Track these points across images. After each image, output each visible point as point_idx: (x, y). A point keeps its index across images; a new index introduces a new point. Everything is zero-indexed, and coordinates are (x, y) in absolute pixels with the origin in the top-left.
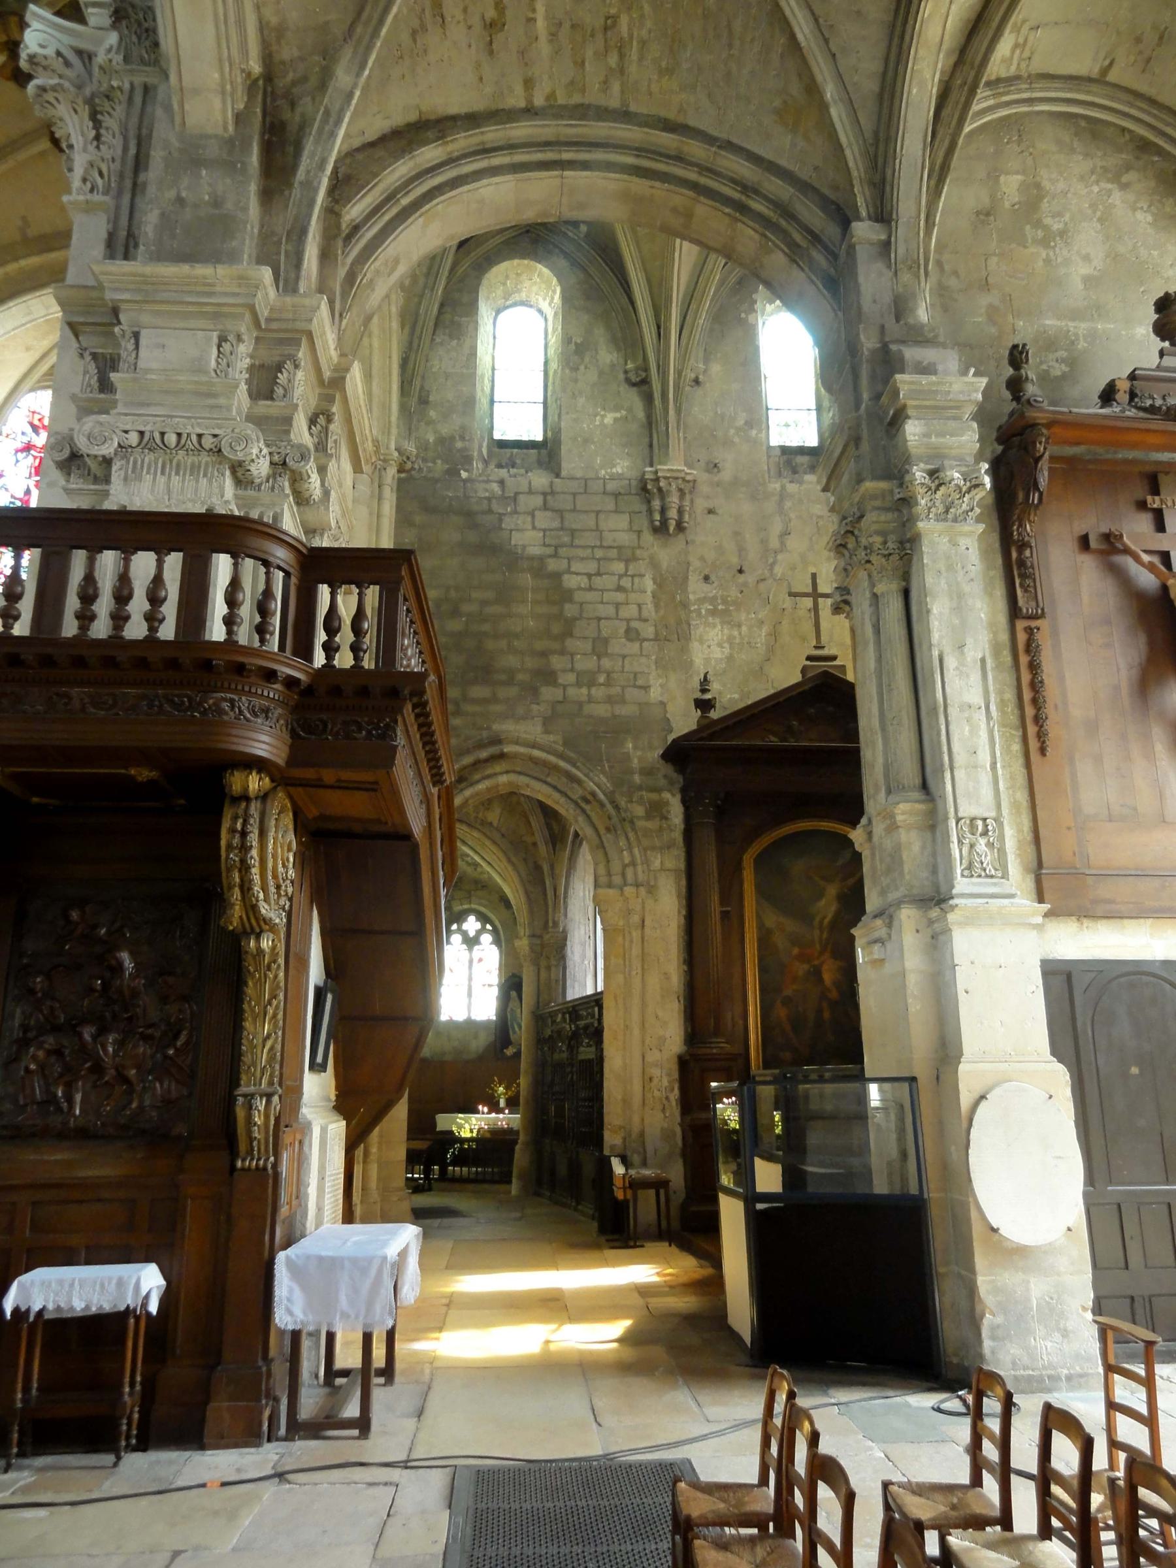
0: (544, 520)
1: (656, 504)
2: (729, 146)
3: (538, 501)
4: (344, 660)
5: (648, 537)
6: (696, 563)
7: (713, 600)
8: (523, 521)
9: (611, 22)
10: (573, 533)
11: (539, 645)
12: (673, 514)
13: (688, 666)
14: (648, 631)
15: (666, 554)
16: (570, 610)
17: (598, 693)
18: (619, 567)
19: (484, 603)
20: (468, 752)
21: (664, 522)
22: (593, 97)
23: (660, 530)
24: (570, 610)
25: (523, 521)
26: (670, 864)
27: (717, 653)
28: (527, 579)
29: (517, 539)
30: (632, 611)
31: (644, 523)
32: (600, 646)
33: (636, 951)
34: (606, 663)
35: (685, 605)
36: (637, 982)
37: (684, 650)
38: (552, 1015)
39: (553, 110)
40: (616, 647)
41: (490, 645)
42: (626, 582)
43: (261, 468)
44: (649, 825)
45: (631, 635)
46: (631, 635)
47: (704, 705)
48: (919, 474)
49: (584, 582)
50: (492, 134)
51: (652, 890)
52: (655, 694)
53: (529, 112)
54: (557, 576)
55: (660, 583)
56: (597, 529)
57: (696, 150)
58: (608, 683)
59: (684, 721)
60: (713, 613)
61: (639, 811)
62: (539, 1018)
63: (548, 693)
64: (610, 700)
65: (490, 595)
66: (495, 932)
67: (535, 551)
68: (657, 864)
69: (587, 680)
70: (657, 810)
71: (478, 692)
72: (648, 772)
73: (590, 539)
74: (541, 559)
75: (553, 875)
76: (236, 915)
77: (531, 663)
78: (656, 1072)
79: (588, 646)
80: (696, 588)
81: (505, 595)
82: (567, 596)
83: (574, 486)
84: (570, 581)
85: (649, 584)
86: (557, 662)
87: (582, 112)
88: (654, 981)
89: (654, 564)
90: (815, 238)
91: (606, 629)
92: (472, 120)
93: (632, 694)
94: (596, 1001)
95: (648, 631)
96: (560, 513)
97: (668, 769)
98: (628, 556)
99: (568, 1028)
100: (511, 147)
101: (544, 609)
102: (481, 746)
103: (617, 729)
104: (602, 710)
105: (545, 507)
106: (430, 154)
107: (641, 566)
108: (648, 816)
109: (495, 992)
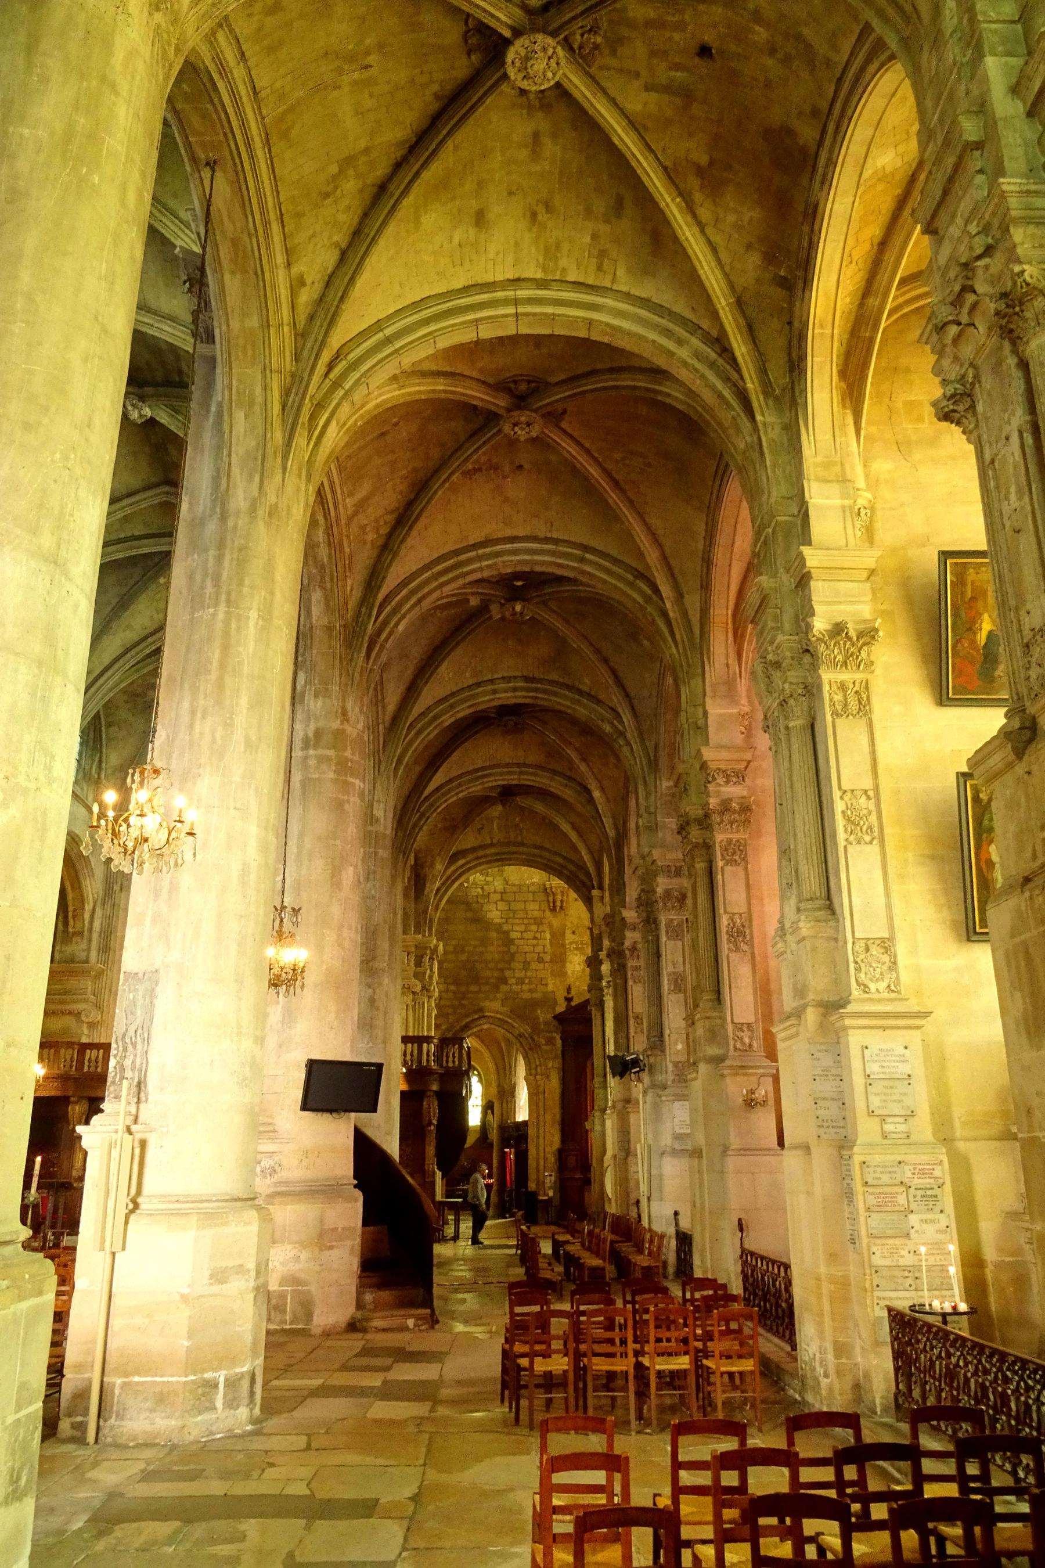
0: (502, 906)
1: (551, 899)
2: (556, 853)
3: (498, 897)
4: (451, 1065)
5: (548, 913)
6: (569, 925)
7: (576, 943)
8: (492, 907)
9: (517, 825)
10: (514, 912)
11: (500, 966)
12: (558, 904)
13: (563, 974)
14: (547, 958)
15: (555, 922)
16: (513, 949)
17: (525, 987)
18: (534, 928)
19: (475, 946)
20: (467, 1016)
21: (554, 907)
22: (512, 839)
23: (553, 909)
24: (513, 949)
25: (492, 907)
26: (556, 1065)
27: (578, 968)
28: (494, 935)
29: (490, 915)
30: (540, 949)
31: (545, 906)
32: (526, 965)
33: (541, 1104)
34: (529, 974)
35: (563, 946)
36: (541, 1118)
37: (564, 966)
38: (509, 1127)
39: (501, 844)
40: (533, 966)
41: (478, 966)
42: (538, 935)
43: (418, 989)
44: (548, 1048)
45: (540, 960)
46: (540, 960)
47: (569, 1000)
48: (604, 983)
49: (519, 935)
50: (481, 853)
51: (548, 1076)
52: (550, 988)
53: (492, 845)
54: (507, 933)
55: (553, 935)
56: (525, 910)
57: (546, 854)
58: (530, 983)
59: (561, 1008)
60: (577, 949)
61: (543, 1042)
62: (503, 1128)
63: (504, 988)
64: (530, 991)
65: (477, 943)
66: (479, 1075)
67: (497, 921)
68: (550, 1065)
69: (521, 981)
70: (550, 1041)
71: (473, 988)
72: (546, 1023)
73: (522, 915)
74: (500, 925)
75: (509, 1053)
76: (426, 1122)
77: (496, 974)
78: (549, 1156)
79: (521, 966)
80: (569, 937)
81: (484, 941)
82: (512, 942)
83: (515, 889)
84: (514, 935)
85: (548, 936)
86: (507, 973)
87: (509, 844)
88: (548, 1117)
89: (551, 926)
90: (584, 884)
91: (529, 957)
92: (474, 849)
93: (540, 988)
94: (525, 1123)
95: (547, 958)
96: (509, 902)
97: (556, 1023)
98: (538, 922)
99: (515, 1134)
100: (485, 856)
101: (502, 949)
102: (475, 1012)
103: (534, 1004)
104: (526, 996)
105: (502, 900)
106: (461, 862)
107: (545, 927)
108: (547, 1044)
109: (480, 1109)
